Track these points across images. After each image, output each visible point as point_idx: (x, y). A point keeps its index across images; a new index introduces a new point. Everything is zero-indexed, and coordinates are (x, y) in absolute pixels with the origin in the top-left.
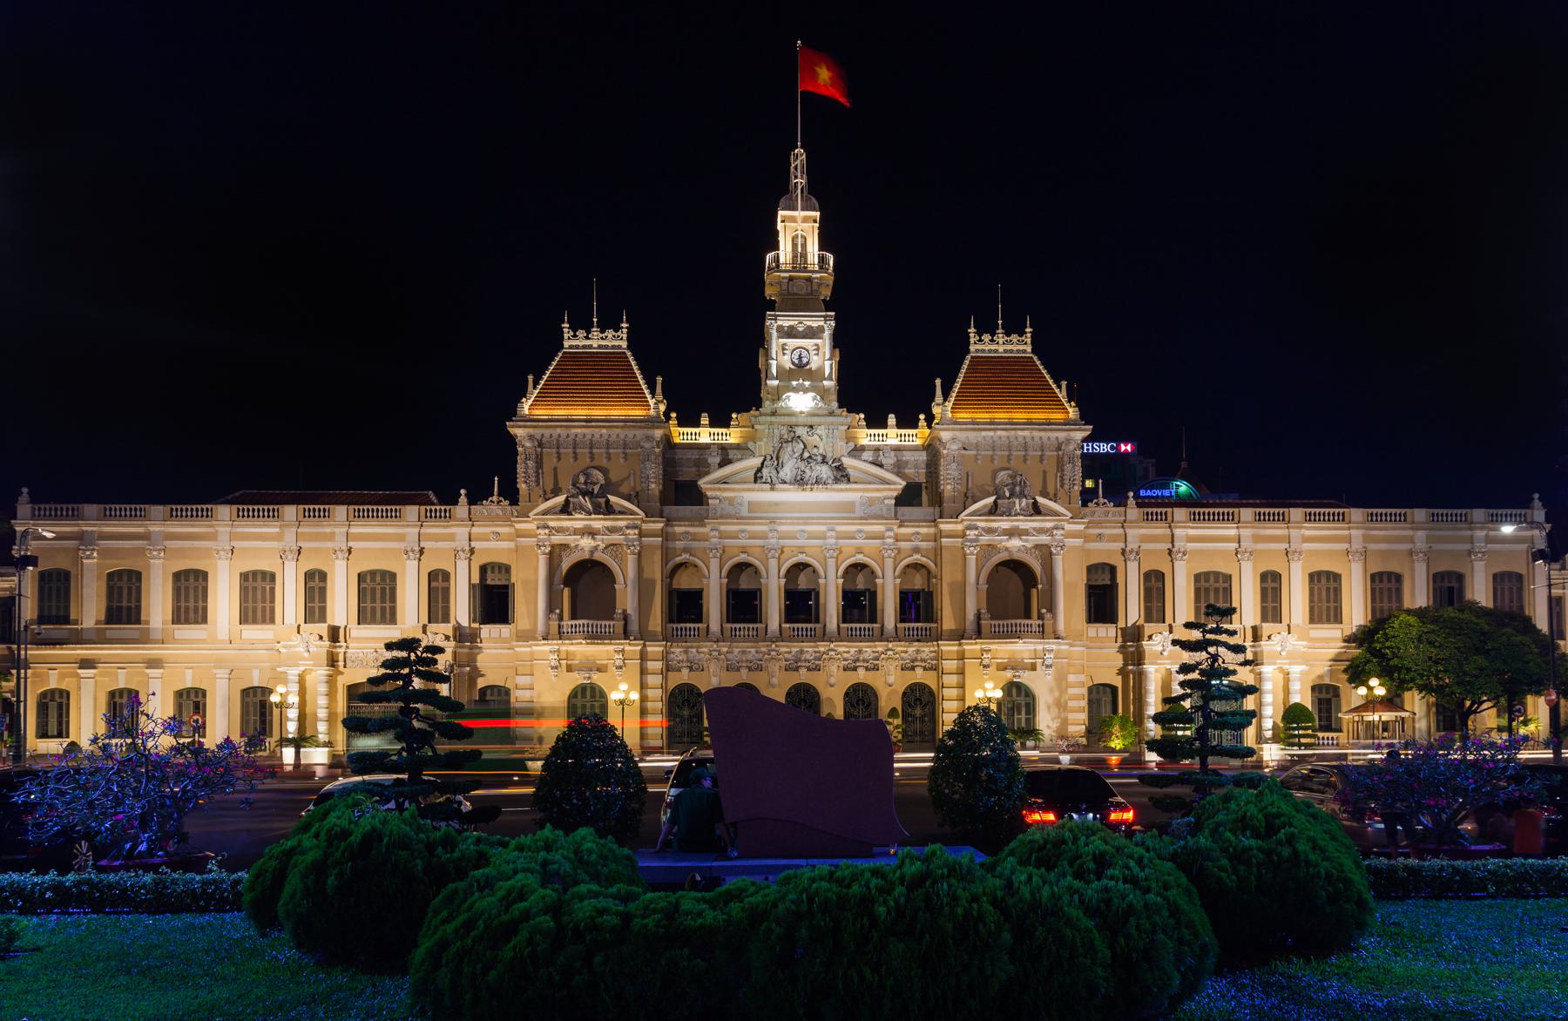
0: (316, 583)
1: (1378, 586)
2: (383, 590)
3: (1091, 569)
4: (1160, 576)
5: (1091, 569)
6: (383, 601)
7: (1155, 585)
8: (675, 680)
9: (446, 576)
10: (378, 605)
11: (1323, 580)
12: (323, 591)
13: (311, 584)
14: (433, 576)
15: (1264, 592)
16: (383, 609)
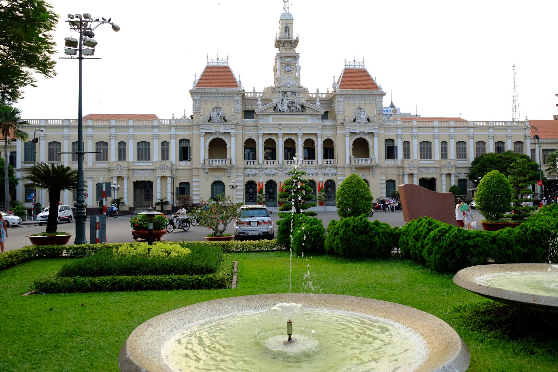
0: (122, 146)
1: (478, 146)
2: (145, 149)
3: (387, 140)
4: (408, 142)
5: (387, 140)
6: (145, 153)
7: (407, 144)
8: (248, 179)
9: (167, 143)
10: (144, 154)
11: (461, 144)
12: (124, 149)
13: (120, 147)
14: (163, 143)
15: (442, 148)
16: (145, 155)
